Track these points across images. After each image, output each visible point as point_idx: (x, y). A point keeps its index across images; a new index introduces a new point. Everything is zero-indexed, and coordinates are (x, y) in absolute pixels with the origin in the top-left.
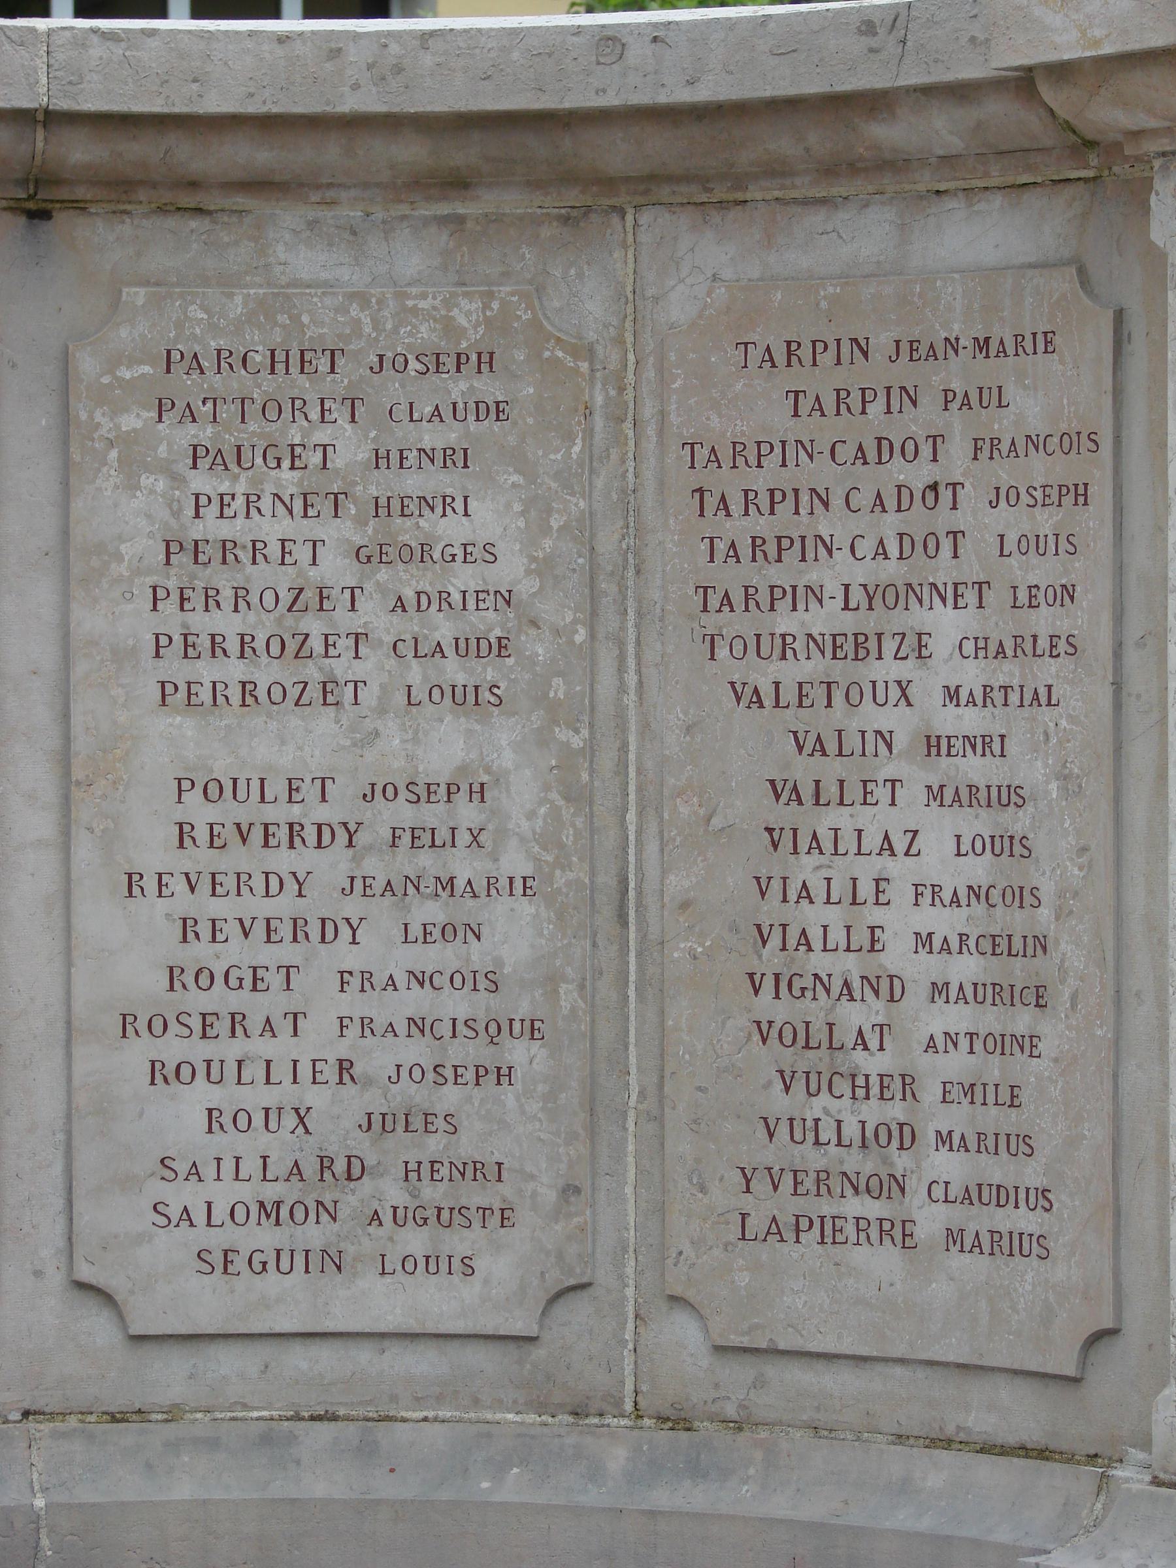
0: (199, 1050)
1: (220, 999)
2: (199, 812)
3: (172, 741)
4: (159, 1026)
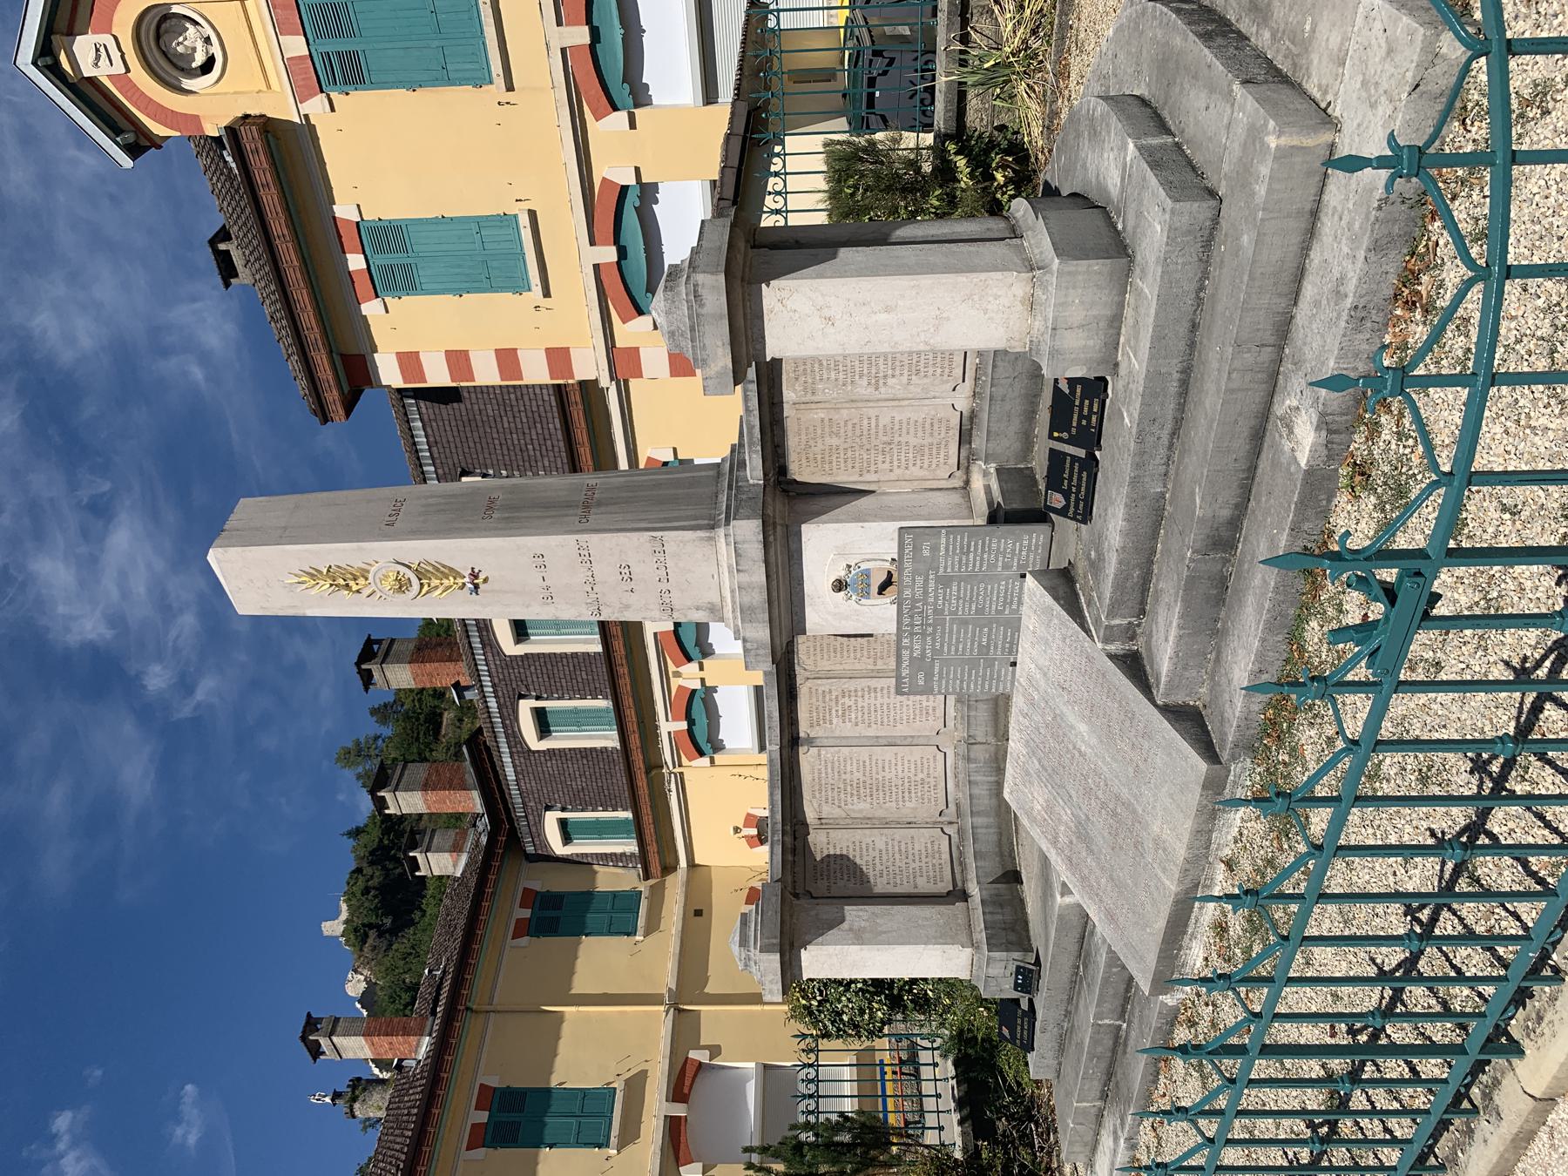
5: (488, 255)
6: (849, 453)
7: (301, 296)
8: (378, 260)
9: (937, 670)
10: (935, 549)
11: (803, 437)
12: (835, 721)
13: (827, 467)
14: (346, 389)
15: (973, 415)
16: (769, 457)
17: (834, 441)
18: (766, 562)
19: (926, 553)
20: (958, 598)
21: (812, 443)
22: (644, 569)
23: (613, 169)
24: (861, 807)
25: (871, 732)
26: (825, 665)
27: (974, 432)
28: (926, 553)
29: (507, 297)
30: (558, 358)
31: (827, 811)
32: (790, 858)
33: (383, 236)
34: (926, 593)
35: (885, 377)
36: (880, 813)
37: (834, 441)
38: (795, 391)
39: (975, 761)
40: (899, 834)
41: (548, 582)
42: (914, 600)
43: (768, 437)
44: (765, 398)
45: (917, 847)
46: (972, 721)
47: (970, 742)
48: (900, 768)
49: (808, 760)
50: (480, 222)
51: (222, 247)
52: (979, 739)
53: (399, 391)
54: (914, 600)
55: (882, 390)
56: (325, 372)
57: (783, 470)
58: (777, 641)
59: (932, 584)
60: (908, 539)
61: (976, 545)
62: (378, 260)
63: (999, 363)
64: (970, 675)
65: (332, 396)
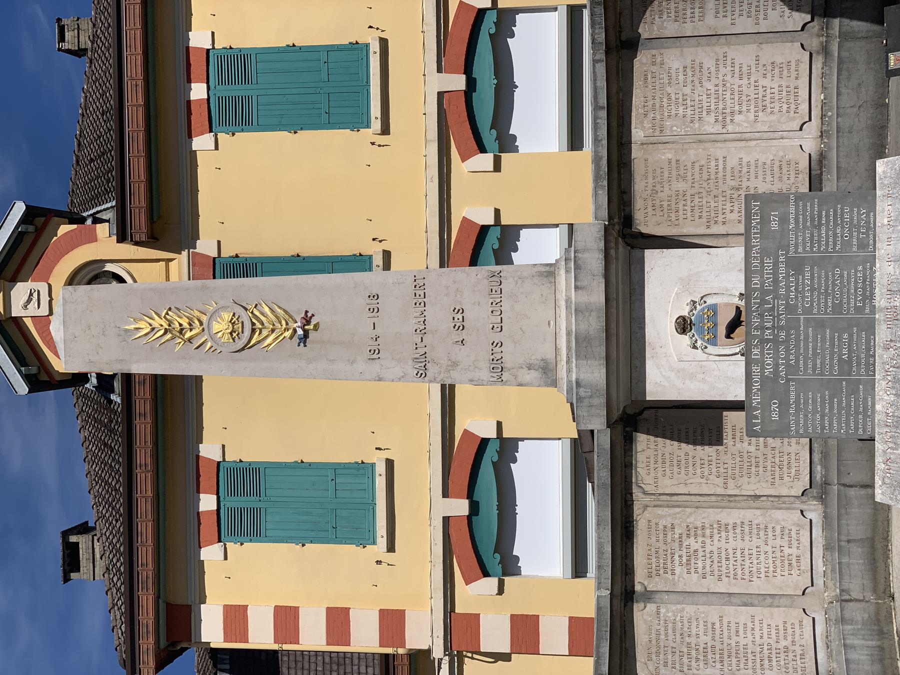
0: (762, 12)
1: (753, 10)
2: (721, 14)
3: (710, 19)
4: (758, 19)
5: (335, 504)
6: (697, 200)
7: (145, 554)
8: (231, 502)
9: (793, 394)
10: (784, 220)
11: (650, 180)
12: (678, 570)
13: (673, 215)
14: (163, 643)
15: (822, 156)
16: (615, 199)
17: (681, 186)
18: (607, 277)
19: (774, 226)
20: (812, 290)
21: (658, 188)
22: (479, 314)
23: (476, 421)
25: (721, 588)
26: (667, 485)
27: (824, 177)
28: (774, 226)
29: (350, 550)
30: (392, 622)
33: (242, 477)
34: (776, 281)
35: (732, 113)
37: (681, 186)
38: (643, 129)
39: (851, 622)
41: (378, 331)
42: (764, 292)
43: (615, 183)
44: (614, 132)
46: (845, 571)
47: (844, 599)
48: (757, 634)
49: (643, 617)
50: (337, 469)
51: (73, 539)
52: (855, 595)
53: (215, 654)
54: (764, 292)
55: (730, 128)
56: (147, 616)
57: (628, 220)
59: (782, 269)
60: (755, 205)
61: (827, 216)
62: (231, 502)
63: (843, 90)
64: (831, 408)
65: (147, 644)
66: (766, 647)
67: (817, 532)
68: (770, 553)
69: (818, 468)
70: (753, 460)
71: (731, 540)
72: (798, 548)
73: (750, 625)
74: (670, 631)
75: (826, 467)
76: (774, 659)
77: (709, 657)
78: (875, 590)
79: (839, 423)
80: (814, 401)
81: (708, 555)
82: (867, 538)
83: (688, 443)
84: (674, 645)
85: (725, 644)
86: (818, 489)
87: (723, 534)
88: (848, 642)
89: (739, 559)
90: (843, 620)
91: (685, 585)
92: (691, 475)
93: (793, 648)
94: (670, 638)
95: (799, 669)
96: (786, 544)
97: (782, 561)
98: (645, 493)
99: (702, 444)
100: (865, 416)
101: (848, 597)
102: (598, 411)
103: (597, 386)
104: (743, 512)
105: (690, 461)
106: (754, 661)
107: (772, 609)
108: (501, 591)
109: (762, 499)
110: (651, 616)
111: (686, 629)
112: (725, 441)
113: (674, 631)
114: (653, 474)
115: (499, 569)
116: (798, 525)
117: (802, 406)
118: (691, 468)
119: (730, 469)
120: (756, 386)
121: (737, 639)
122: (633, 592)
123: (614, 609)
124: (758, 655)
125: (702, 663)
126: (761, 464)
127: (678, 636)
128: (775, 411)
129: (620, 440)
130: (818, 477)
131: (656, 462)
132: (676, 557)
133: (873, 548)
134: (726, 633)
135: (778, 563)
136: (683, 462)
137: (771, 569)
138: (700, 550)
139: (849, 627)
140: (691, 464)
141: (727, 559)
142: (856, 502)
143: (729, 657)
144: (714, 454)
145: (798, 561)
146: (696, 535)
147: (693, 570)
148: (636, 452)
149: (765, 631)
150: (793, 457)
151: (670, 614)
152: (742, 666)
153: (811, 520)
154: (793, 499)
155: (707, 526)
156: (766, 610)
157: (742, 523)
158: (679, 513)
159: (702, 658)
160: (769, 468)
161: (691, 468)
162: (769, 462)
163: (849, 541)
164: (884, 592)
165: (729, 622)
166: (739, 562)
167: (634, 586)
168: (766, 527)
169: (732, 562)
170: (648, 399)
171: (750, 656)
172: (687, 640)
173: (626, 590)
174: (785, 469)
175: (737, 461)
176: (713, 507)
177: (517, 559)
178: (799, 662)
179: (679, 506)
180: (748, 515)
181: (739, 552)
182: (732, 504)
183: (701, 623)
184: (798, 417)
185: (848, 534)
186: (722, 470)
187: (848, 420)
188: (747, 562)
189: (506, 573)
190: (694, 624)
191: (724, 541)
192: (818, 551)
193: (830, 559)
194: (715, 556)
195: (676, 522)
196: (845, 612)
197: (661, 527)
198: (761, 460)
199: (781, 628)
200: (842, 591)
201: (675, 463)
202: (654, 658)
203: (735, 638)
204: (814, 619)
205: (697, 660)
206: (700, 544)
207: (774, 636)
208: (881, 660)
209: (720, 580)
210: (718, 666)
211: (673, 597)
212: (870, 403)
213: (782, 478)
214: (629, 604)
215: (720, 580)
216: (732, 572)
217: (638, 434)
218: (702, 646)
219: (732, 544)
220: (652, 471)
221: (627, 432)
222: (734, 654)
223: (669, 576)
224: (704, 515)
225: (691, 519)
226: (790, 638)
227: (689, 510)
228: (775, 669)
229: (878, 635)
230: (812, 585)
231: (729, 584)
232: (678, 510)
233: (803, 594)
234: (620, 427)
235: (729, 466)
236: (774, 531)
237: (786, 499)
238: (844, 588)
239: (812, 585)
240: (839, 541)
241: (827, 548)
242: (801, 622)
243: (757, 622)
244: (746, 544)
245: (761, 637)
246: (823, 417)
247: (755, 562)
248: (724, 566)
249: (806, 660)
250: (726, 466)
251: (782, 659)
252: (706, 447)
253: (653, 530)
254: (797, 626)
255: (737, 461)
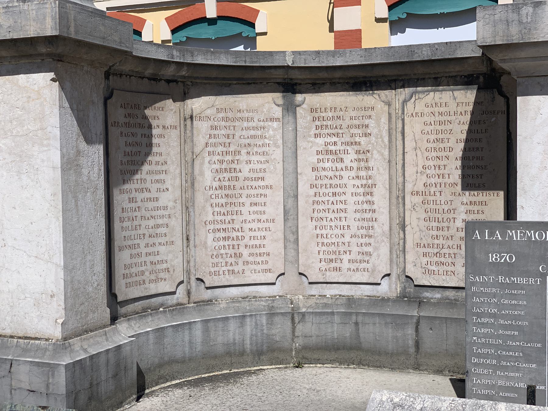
9: (522, 281)
12: (320, 141)
24: (207, 175)
25: (303, 188)
26: (414, 128)
31: (202, 127)
32: (149, 72)
36: (200, 199)
39: (270, 323)
40: (176, 224)
45: (162, 249)
46: (324, 319)
47: (295, 316)
48: (254, 225)
49: (267, 103)
52: (300, 328)
58: (523, 54)
64: (505, 327)
66: (240, 234)
67: (367, 290)
68: (342, 240)
69: (437, 295)
70: (445, 224)
71: (355, 198)
72: (349, 269)
73: (263, 217)
74: (252, 132)
75: (439, 303)
76: (226, 243)
77: (225, 175)
78: (305, 348)
79: (486, 336)
80: (515, 307)
81: (338, 174)
82: (360, 343)
83: (465, 150)
84: (237, 137)
85: (241, 192)
86: (414, 293)
87: (361, 190)
88: (248, 320)
89: (335, 207)
90: (272, 314)
91: (305, 148)
92: (427, 154)
93: (240, 263)
94: (244, 133)
95: (216, 269)
96: (353, 256)
97: (335, 253)
98: (405, 102)
99: (463, 167)
100: (496, 368)
101: (297, 320)
102: (501, 34)
103: (536, 29)
104: (386, 211)
105: (443, 154)
106: (223, 222)
107: (282, 241)
108: (378, 20)
109: (401, 233)
110: (269, 111)
111: (256, 149)
112: (467, 193)
113: (253, 137)
114: (427, 110)
115: (395, 18)
116: (373, 271)
117: (507, 291)
118: (434, 154)
119: (433, 198)
120: (535, 236)
121: (248, 204)
122: (295, 92)
123: (273, 71)
124: (230, 226)
125: (217, 166)
126: (440, 233)
127: (247, 141)
128: (501, 258)
129: (468, 69)
130: (427, 294)
131: (441, 114)
132: (334, 139)
133: (351, 348)
134: (253, 192)
135: (332, 248)
136: (442, 146)
137: (326, 241)
138: (343, 165)
139: (264, 320)
140: (440, 154)
141: (334, 194)
142: (399, 335)
143: (227, 196)
144: (451, 180)
145: (335, 269)
146: (359, 160)
147: (321, 157)
148: (453, 90)
149: (258, 234)
150: (450, 268)
151: (271, 132)
152: (217, 209)
153: (379, 284)
154: (402, 265)
155: (370, 173)
156: (281, 235)
157: (374, 211)
158: (383, 141)
159: (223, 167)
160: (436, 242)
161: (434, 154)
162: (444, 242)
163: (357, 324)
164: (304, 358)
165: (265, 196)
166: (332, 207)
167: (301, 93)
168: (370, 237)
169: (332, 199)
170: (519, 99)
171: (229, 218)
172: (244, 151)
173: (296, 84)
174: (435, 259)
175: (444, 206)
176: (390, 179)
177: (403, 32)
178: (224, 268)
179: (390, 141)
180: (383, 217)
181: (342, 206)
182: (394, 201)
183: (263, 166)
184: (493, 285)
185: (364, 324)
186: (433, 189)
187: (490, 346)
188: (331, 216)
189: (392, 23)
190: (263, 159)
191: (354, 190)
192: (346, 290)
193: (339, 302)
194: (338, 182)
195: (373, 139)
196: (280, 317)
197: (367, 122)
198: (446, 233)
199: (262, 250)
200: (303, 315)
201: (440, 136)
202: (221, 115)
203: (248, 202)
204: (274, 284)
205: (221, 162)
206: (349, 164)
207: (253, 242)
208: (229, 354)
209: (312, 186)
210: (216, 184)
211: (290, 136)
212: (512, 374)
213: (425, 255)
214: (281, 88)
215: (312, 186)
216: (320, 199)
217: (475, 91)
218: (238, 167)
219: (351, 200)
220: (430, 110)
221: (478, 78)
222: (230, 200)
223: (313, 131)
224: (381, 169)
225: (376, 155)
226: (251, 259)
227: (386, 153)
228: (215, 244)
229: (257, 351)
230: (310, 283)
231: (308, 196)
232: (386, 140)
233: (300, 274)
234: (483, 69)
235: (438, 197)
236: (366, 245)
237: (402, 259)
238: (307, 317)
239: (310, 283)
240: (357, 314)
241: (350, 301)
242: (270, 270)
243: (266, 225)
244: (351, 215)
245: (251, 230)
246: (494, 316)
247: (333, 224)
248: (327, 191)
249: (227, 276)
250: (438, 194)
251: (227, 251)
252: (459, 172)
253: (363, 113)
254: (265, 267)
255: (444, 206)
